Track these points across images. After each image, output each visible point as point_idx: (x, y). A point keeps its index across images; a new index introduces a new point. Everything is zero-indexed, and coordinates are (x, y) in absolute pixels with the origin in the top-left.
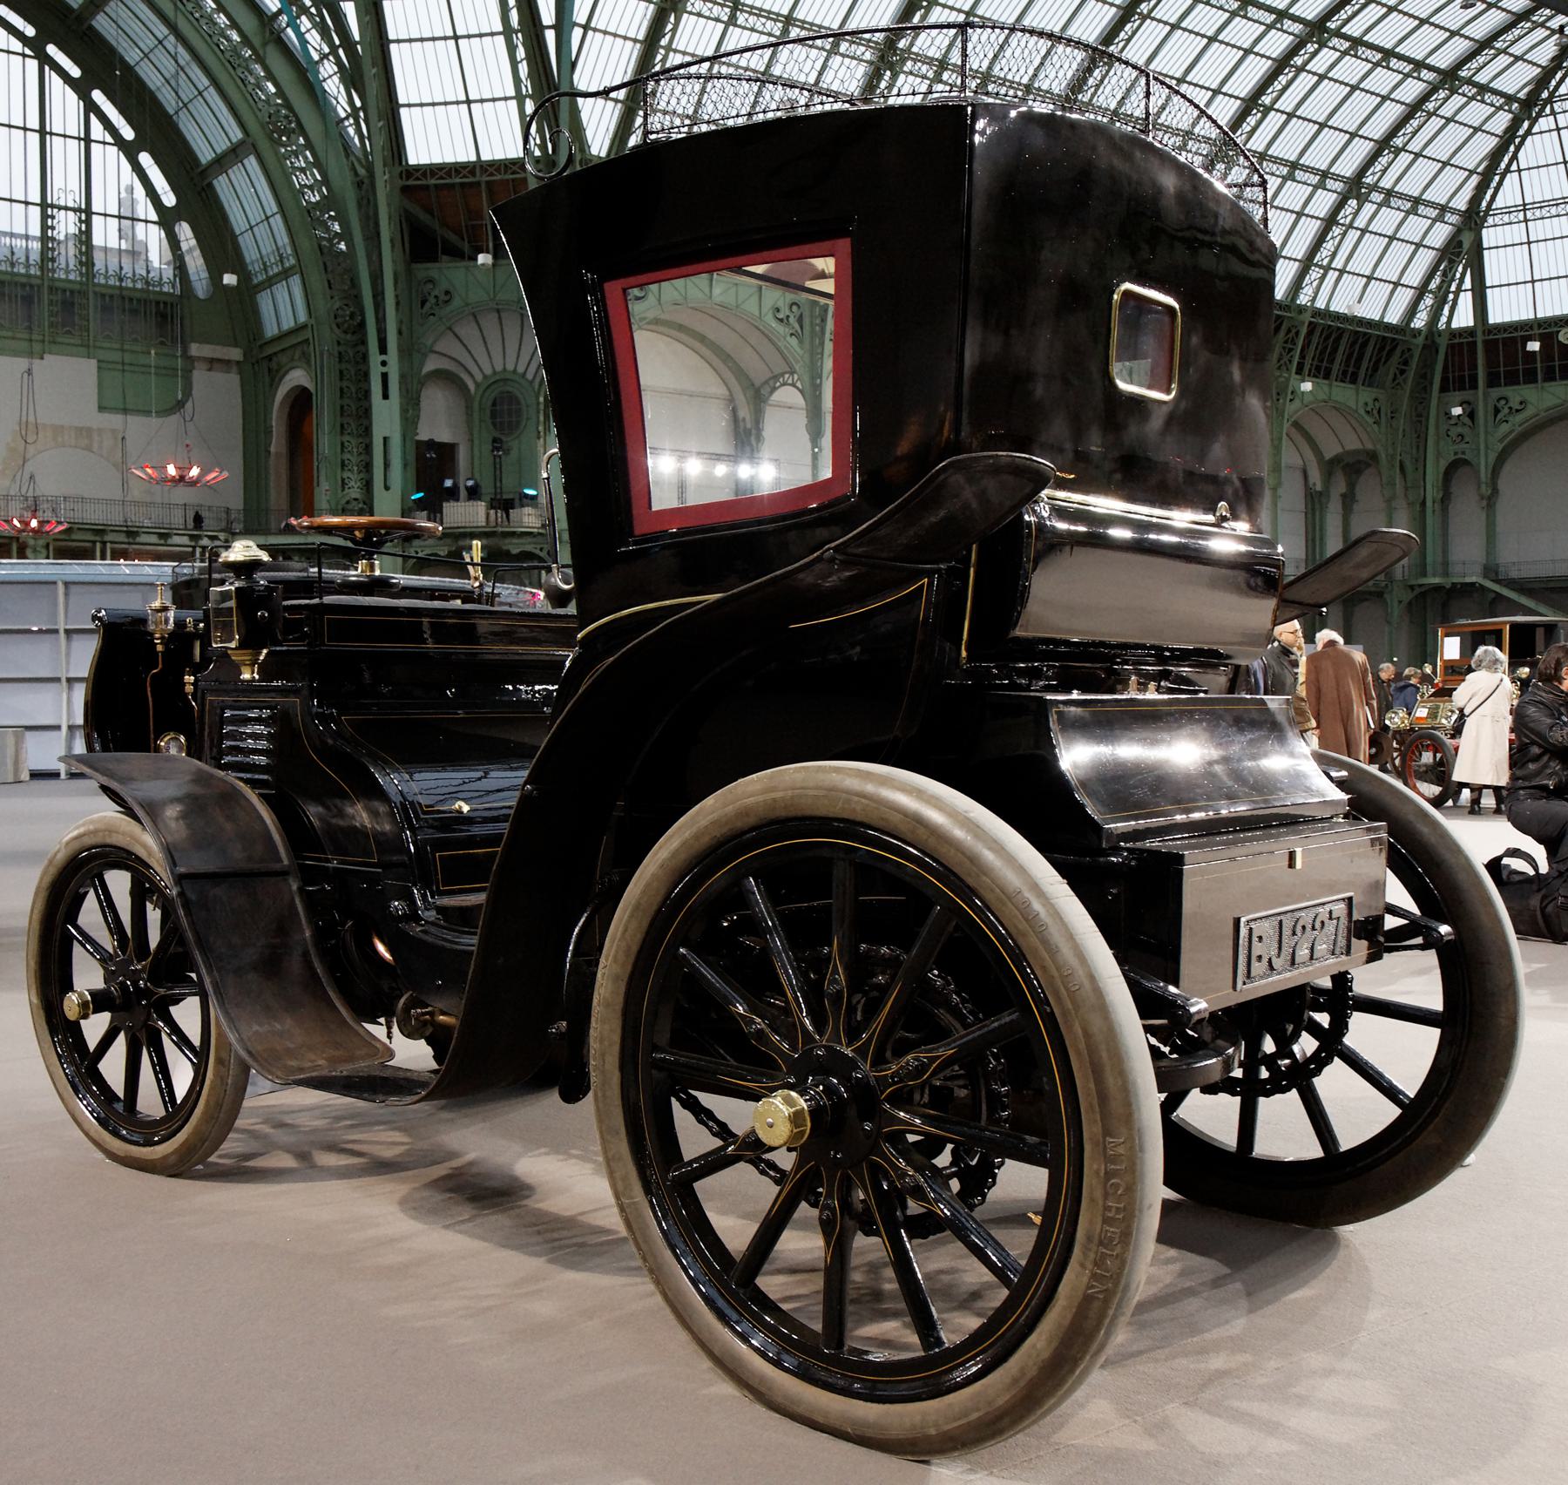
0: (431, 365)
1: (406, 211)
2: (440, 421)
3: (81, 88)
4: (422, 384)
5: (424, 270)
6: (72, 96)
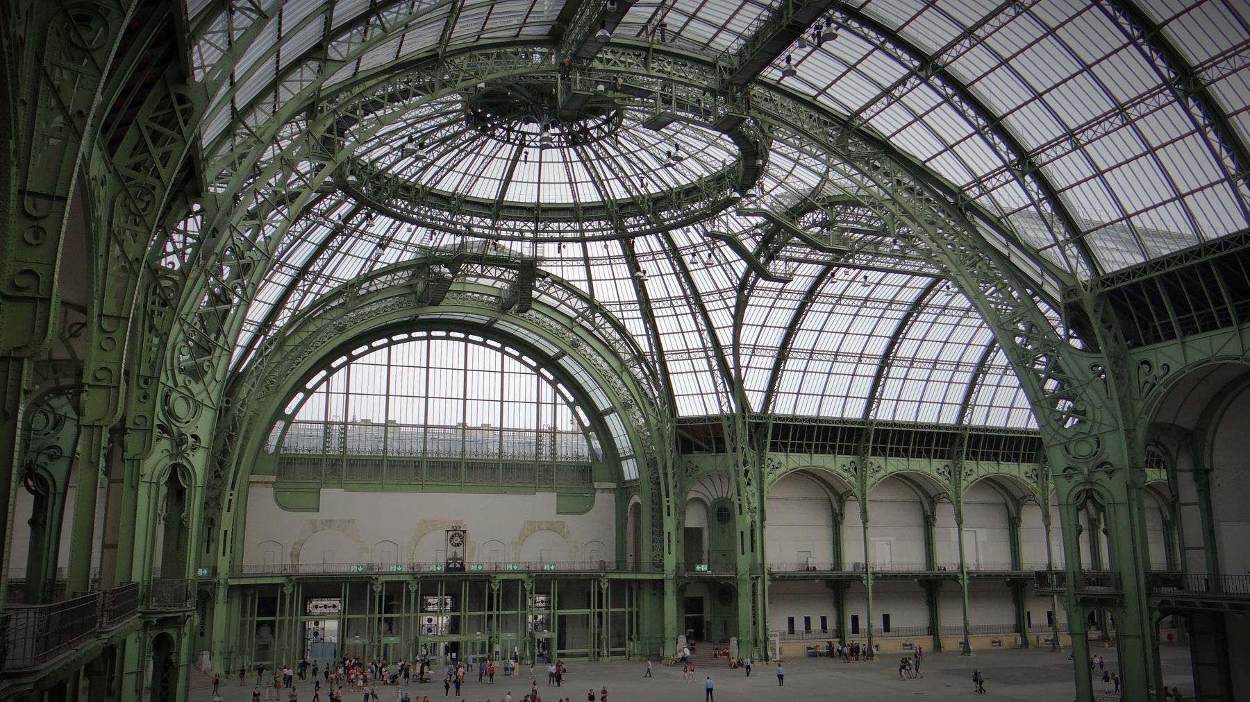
0: (691, 495)
1: (680, 436)
2: (695, 518)
3: (553, 384)
4: (687, 504)
5: (687, 457)
6: (550, 387)
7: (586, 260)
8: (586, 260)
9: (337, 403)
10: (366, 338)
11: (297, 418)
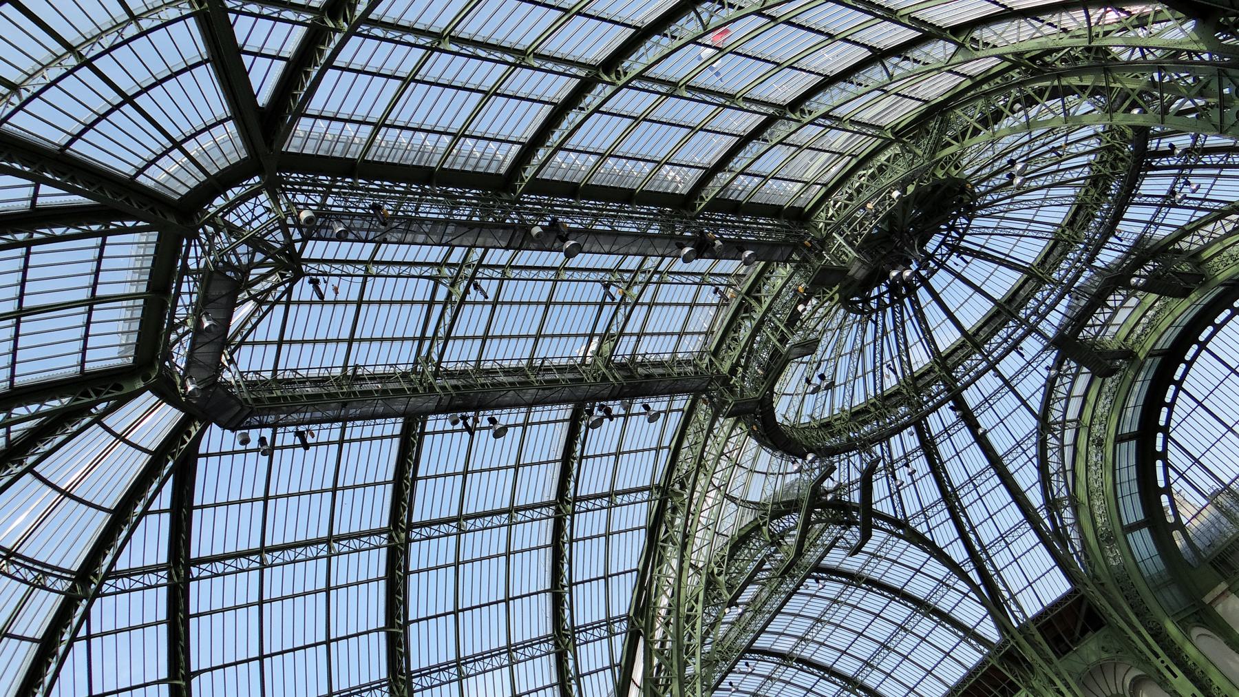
7: (1170, 200)
8: (1170, 200)
9: (1196, 474)
10: (1154, 402)
11: (1184, 521)
